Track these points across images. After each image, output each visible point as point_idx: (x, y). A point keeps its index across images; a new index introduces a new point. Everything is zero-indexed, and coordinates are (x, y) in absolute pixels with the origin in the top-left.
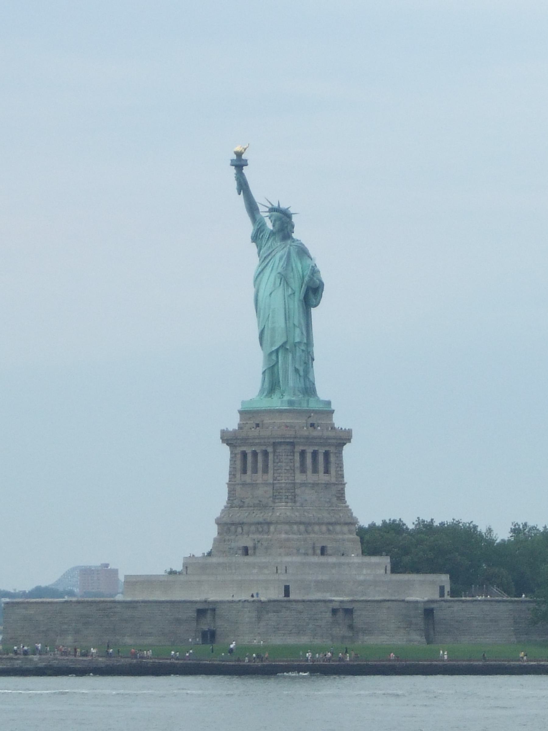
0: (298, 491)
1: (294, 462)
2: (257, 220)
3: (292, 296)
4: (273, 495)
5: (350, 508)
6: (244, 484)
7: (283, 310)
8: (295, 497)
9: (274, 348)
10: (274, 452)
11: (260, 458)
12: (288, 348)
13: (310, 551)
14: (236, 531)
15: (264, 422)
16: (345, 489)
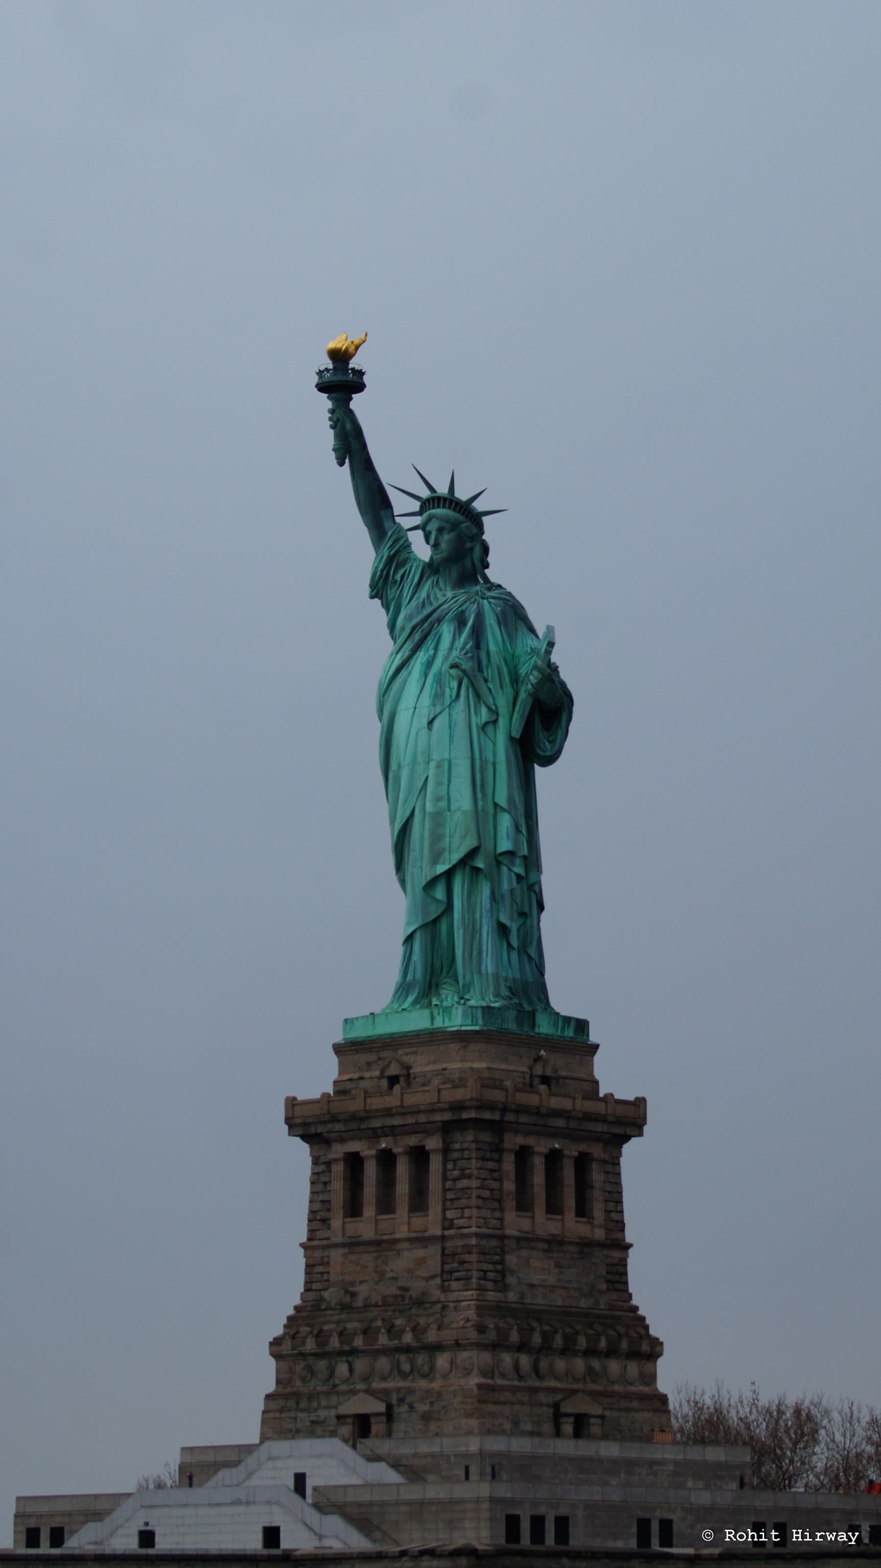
0: (512, 1260)
1: (500, 1180)
2: (389, 534)
3: (490, 729)
4: (443, 1271)
5: (641, 1312)
6: (353, 1244)
7: (468, 763)
8: (504, 1276)
9: (441, 868)
10: (446, 1151)
11: (403, 1168)
12: (480, 864)
13: (548, 1428)
14: (332, 1374)
15: (412, 1071)
16: (629, 1260)
